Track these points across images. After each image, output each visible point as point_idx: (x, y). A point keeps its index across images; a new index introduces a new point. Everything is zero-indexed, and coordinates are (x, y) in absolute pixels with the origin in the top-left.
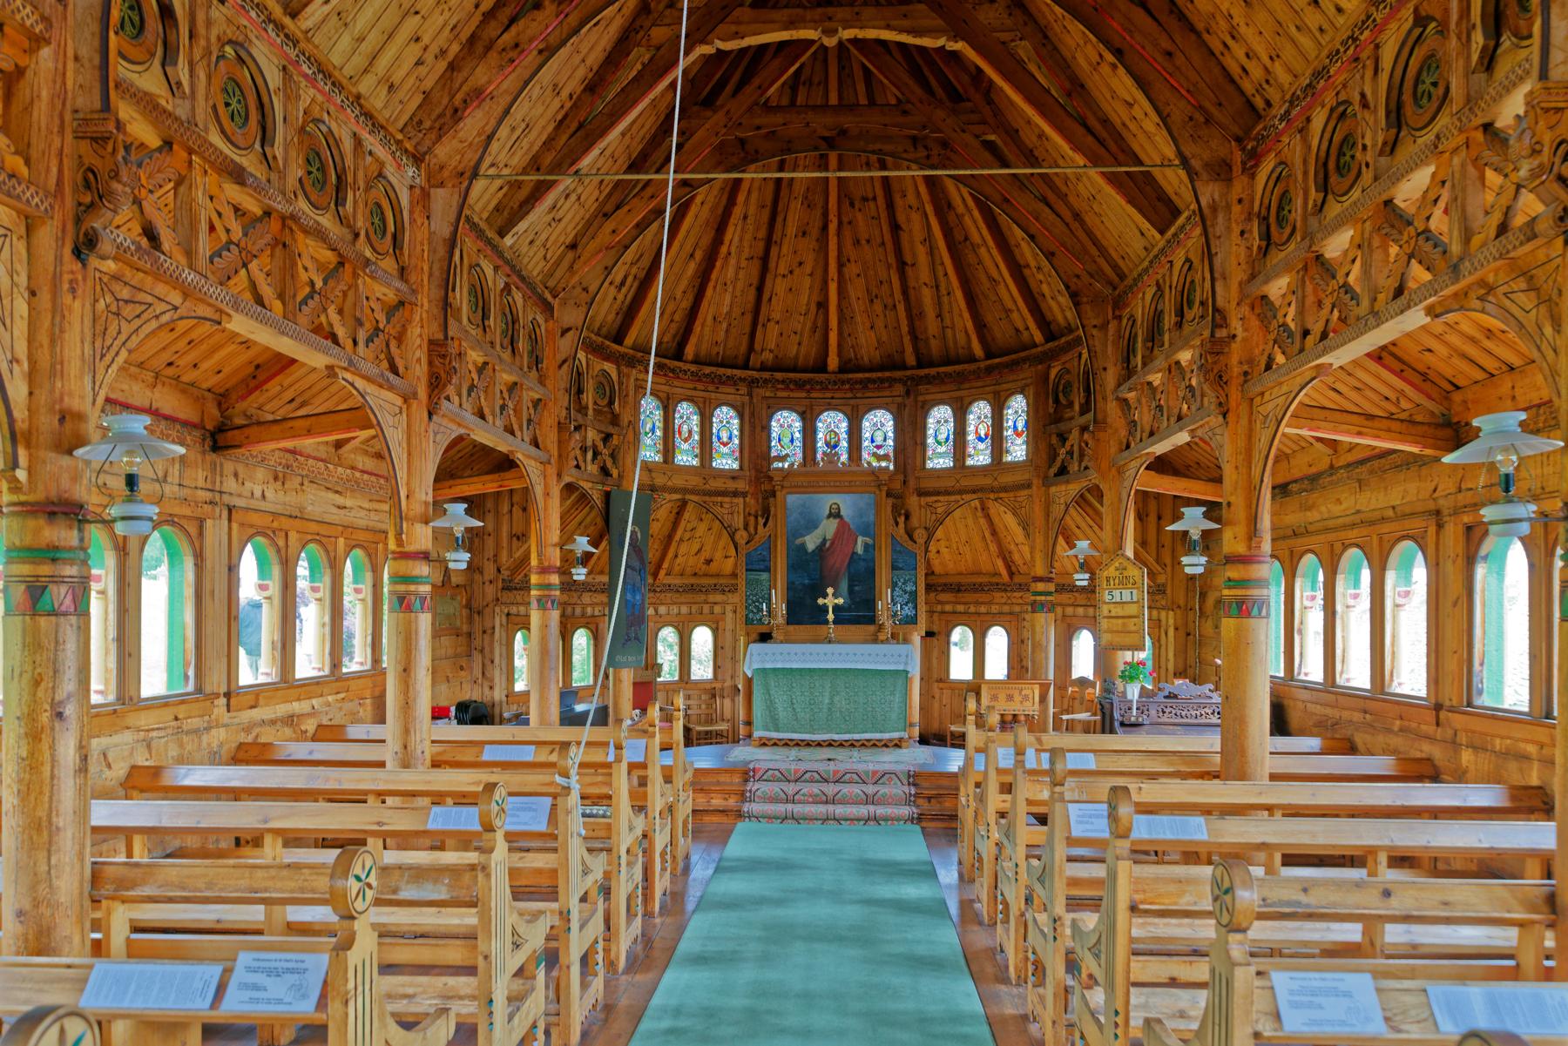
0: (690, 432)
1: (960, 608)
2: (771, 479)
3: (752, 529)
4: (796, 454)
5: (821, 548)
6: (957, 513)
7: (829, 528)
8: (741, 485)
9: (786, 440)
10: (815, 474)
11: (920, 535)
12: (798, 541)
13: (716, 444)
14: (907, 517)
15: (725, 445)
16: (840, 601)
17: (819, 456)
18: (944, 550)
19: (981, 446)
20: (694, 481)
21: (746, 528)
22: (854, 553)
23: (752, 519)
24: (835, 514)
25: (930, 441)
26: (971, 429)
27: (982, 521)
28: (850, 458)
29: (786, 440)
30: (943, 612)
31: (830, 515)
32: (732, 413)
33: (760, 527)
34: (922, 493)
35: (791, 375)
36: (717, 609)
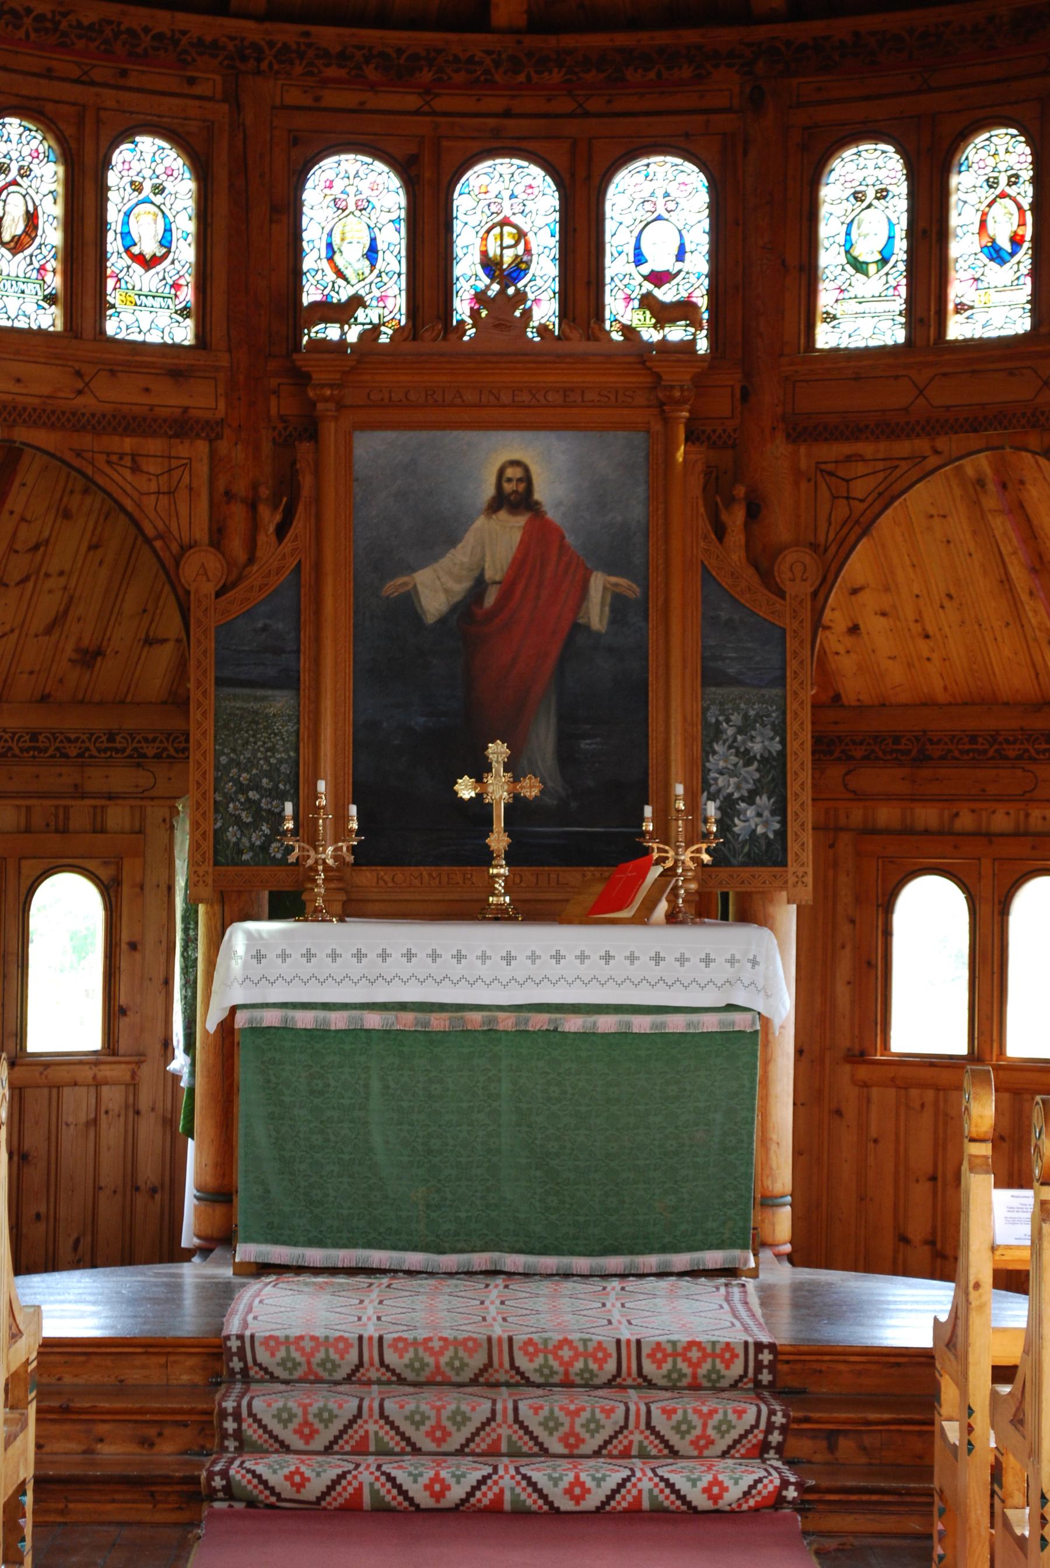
0: (31, 219)
1: (927, 816)
2: (301, 379)
3: (236, 546)
4: (388, 304)
5: (468, 609)
6: (920, 498)
7: (494, 543)
8: (203, 400)
9: (352, 259)
10: (449, 361)
11: (796, 569)
12: (393, 587)
13: (117, 261)
14: (754, 511)
15: (149, 263)
16: (531, 789)
17: (462, 308)
18: (874, 625)
19: (999, 274)
20: (44, 382)
21: (218, 537)
22: (579, 628)
23: (238, 514)
24: (515, 497)
25: (830, 258)
26: (962, 218)
27: (1000, 525)
28: (565, 313)
29: (352, 259)
30: (869, 831)
31: (500, 502)
32: (173, 159)
33: (266, 537)
34: (803, 430)
35: (372, 36)
36: (117, 816)
